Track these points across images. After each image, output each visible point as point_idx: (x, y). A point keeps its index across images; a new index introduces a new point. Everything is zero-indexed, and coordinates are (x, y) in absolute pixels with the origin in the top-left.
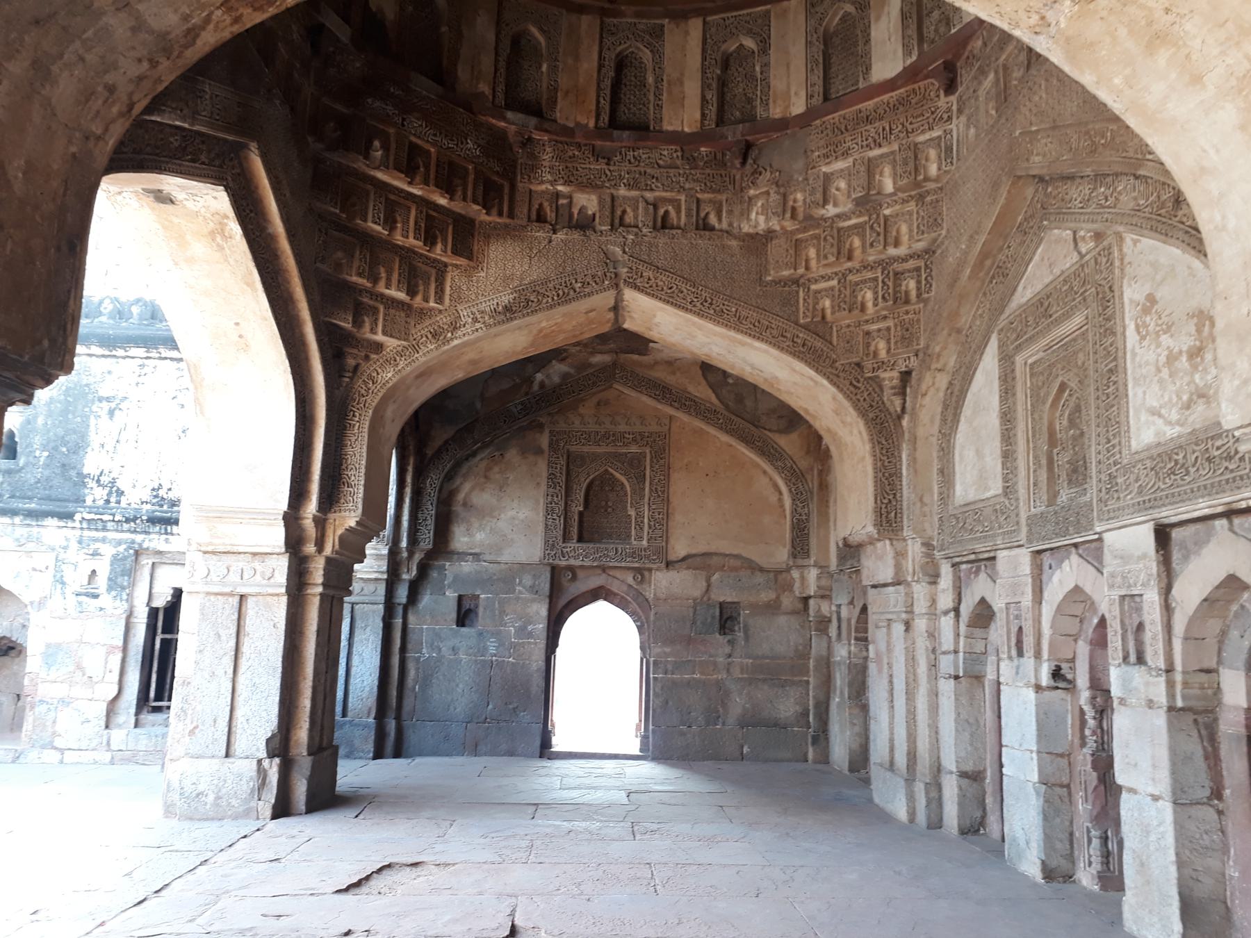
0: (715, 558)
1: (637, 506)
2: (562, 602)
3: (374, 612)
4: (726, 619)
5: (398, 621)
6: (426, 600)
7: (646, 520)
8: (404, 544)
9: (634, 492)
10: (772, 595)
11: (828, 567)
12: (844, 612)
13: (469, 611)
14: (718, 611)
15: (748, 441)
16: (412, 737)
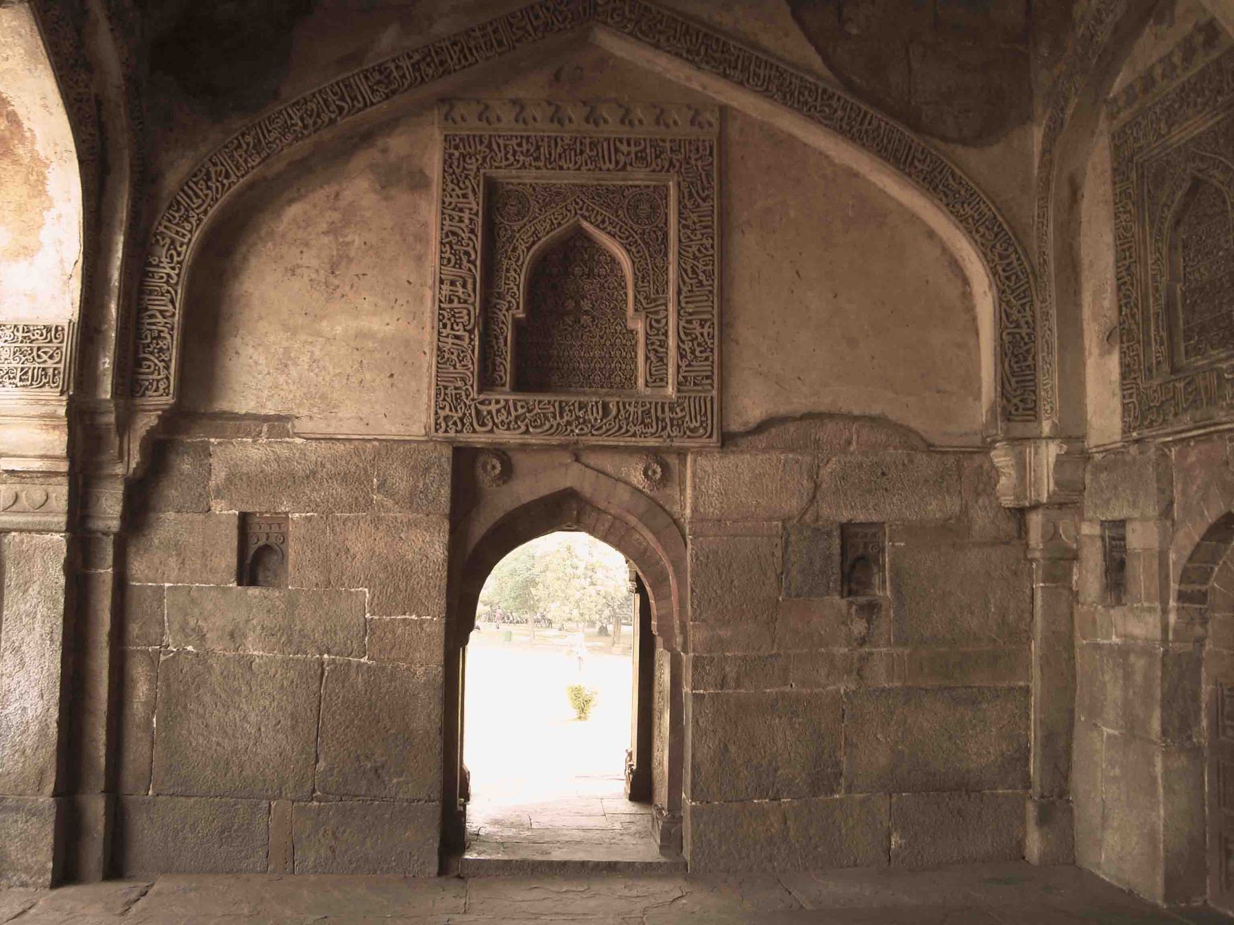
0: (830, 426)
1: (651, 306)
2: (481, 527)
3: (45, 550)
4: (855, 559)
5: (106, 572)
6: (170, 523)
7: (672, 342)
8: (106, 391)
9: (641, 276)
10: (953, 505)
11: (1082, 438)
12: (1140, 538)
13: (267, 549)
14: (837, 542)
15: (901, 160)
16: (147, 833)
